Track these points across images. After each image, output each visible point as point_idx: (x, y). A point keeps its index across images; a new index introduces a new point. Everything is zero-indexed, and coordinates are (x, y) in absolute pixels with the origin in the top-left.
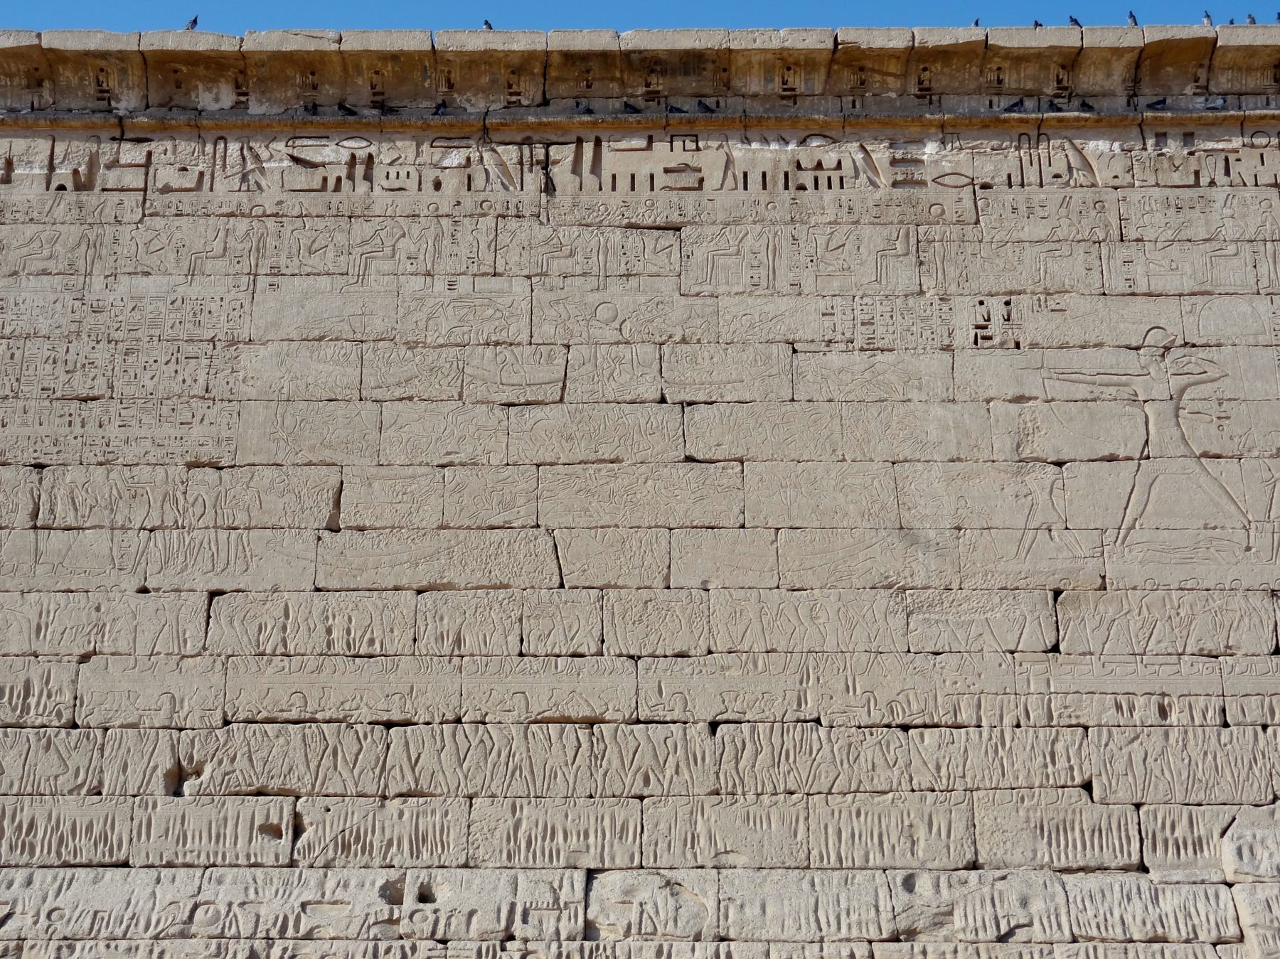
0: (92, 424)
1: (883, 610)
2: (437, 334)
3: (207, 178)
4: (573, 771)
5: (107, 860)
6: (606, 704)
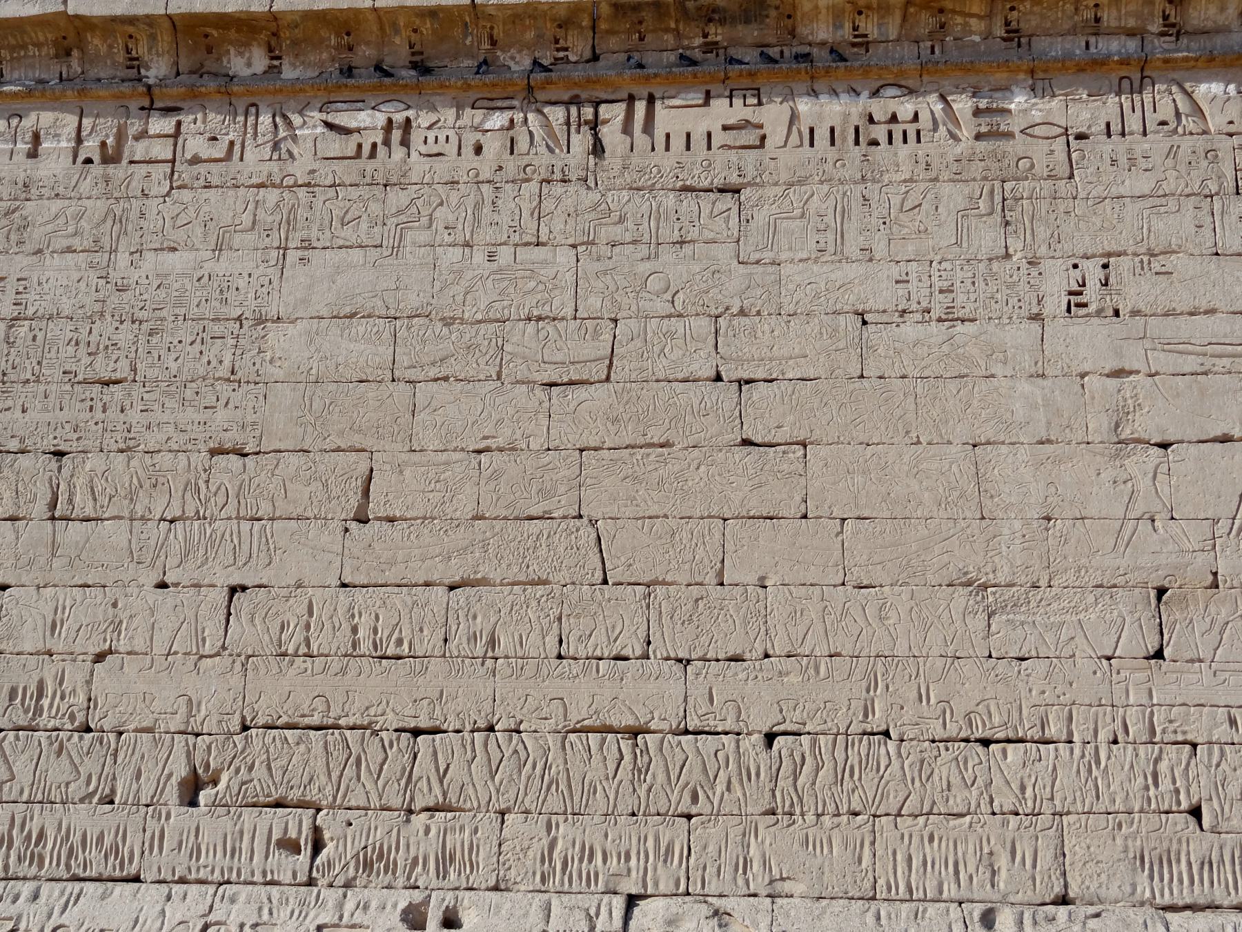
0: (114, 408)
1: (961, 610)
3: (237, 148)
4: (615, 786)
5: (117, 874)
6: (652, 712)
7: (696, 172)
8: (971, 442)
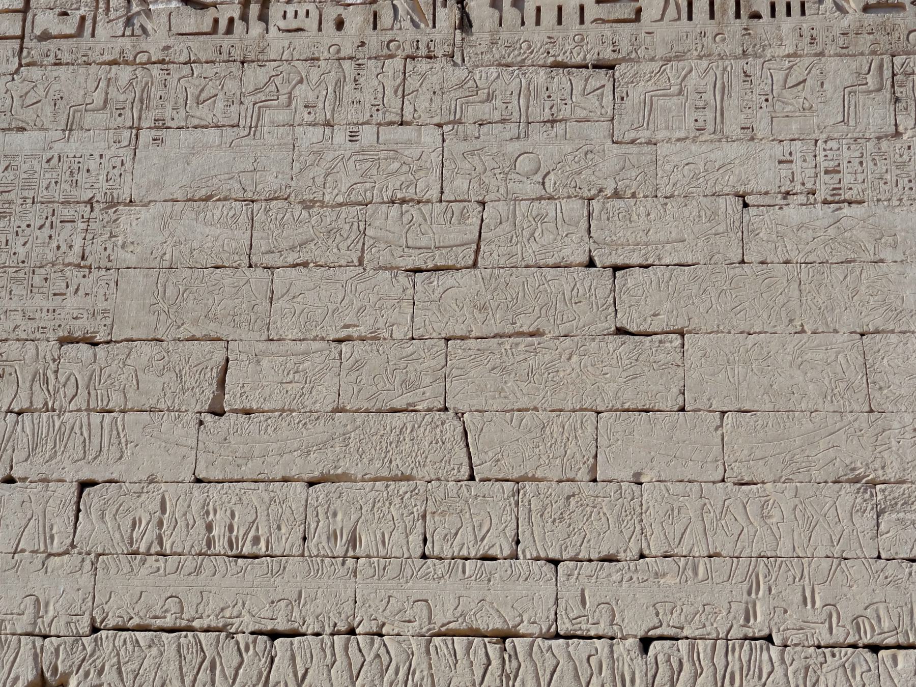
1: (848, 508)
2: (336, 191)
3: (88, 23)
6: (521, 615)
7: (567, 47)
8: (858, 330)
